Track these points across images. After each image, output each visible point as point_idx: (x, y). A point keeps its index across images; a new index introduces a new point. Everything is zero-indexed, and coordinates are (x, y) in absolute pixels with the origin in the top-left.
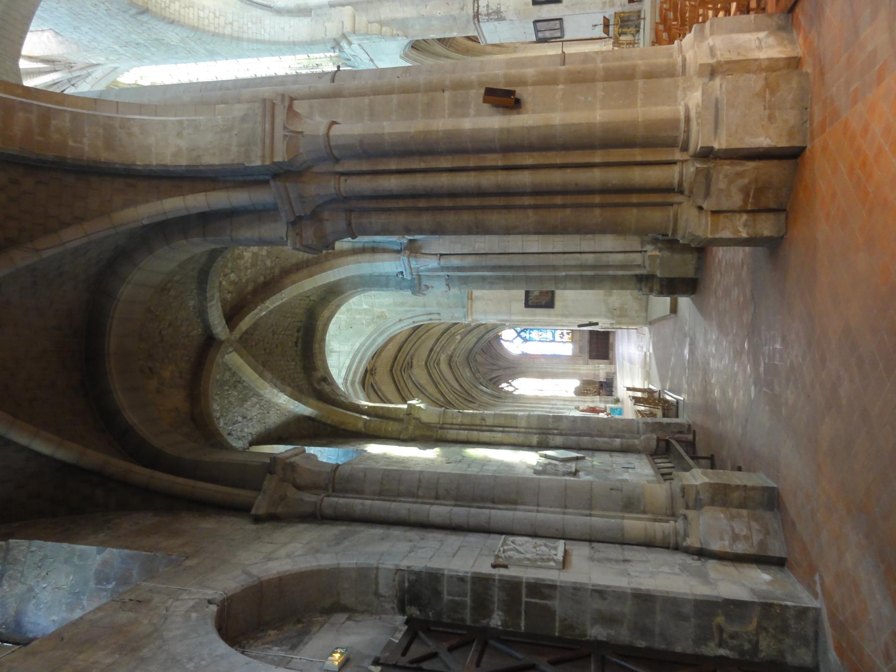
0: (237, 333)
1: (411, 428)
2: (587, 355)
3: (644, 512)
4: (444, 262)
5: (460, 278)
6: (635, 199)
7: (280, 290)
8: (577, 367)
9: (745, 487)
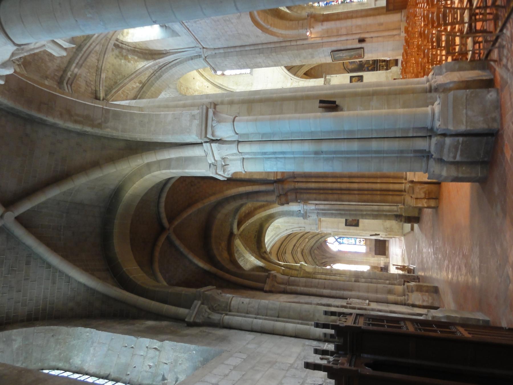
0: (239, 232)
1: (302, 273)
2: (373, 253)
3: (395, 294)
4: (317, 207)
5: (323, 213)
6: (391, 193)
7: (254, 216)
8: (368, 258)
9: (427, 286)
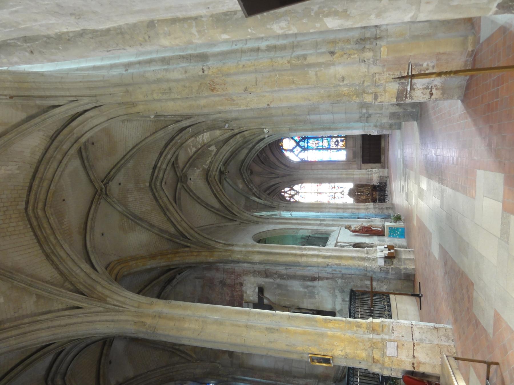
8: (350, 172)
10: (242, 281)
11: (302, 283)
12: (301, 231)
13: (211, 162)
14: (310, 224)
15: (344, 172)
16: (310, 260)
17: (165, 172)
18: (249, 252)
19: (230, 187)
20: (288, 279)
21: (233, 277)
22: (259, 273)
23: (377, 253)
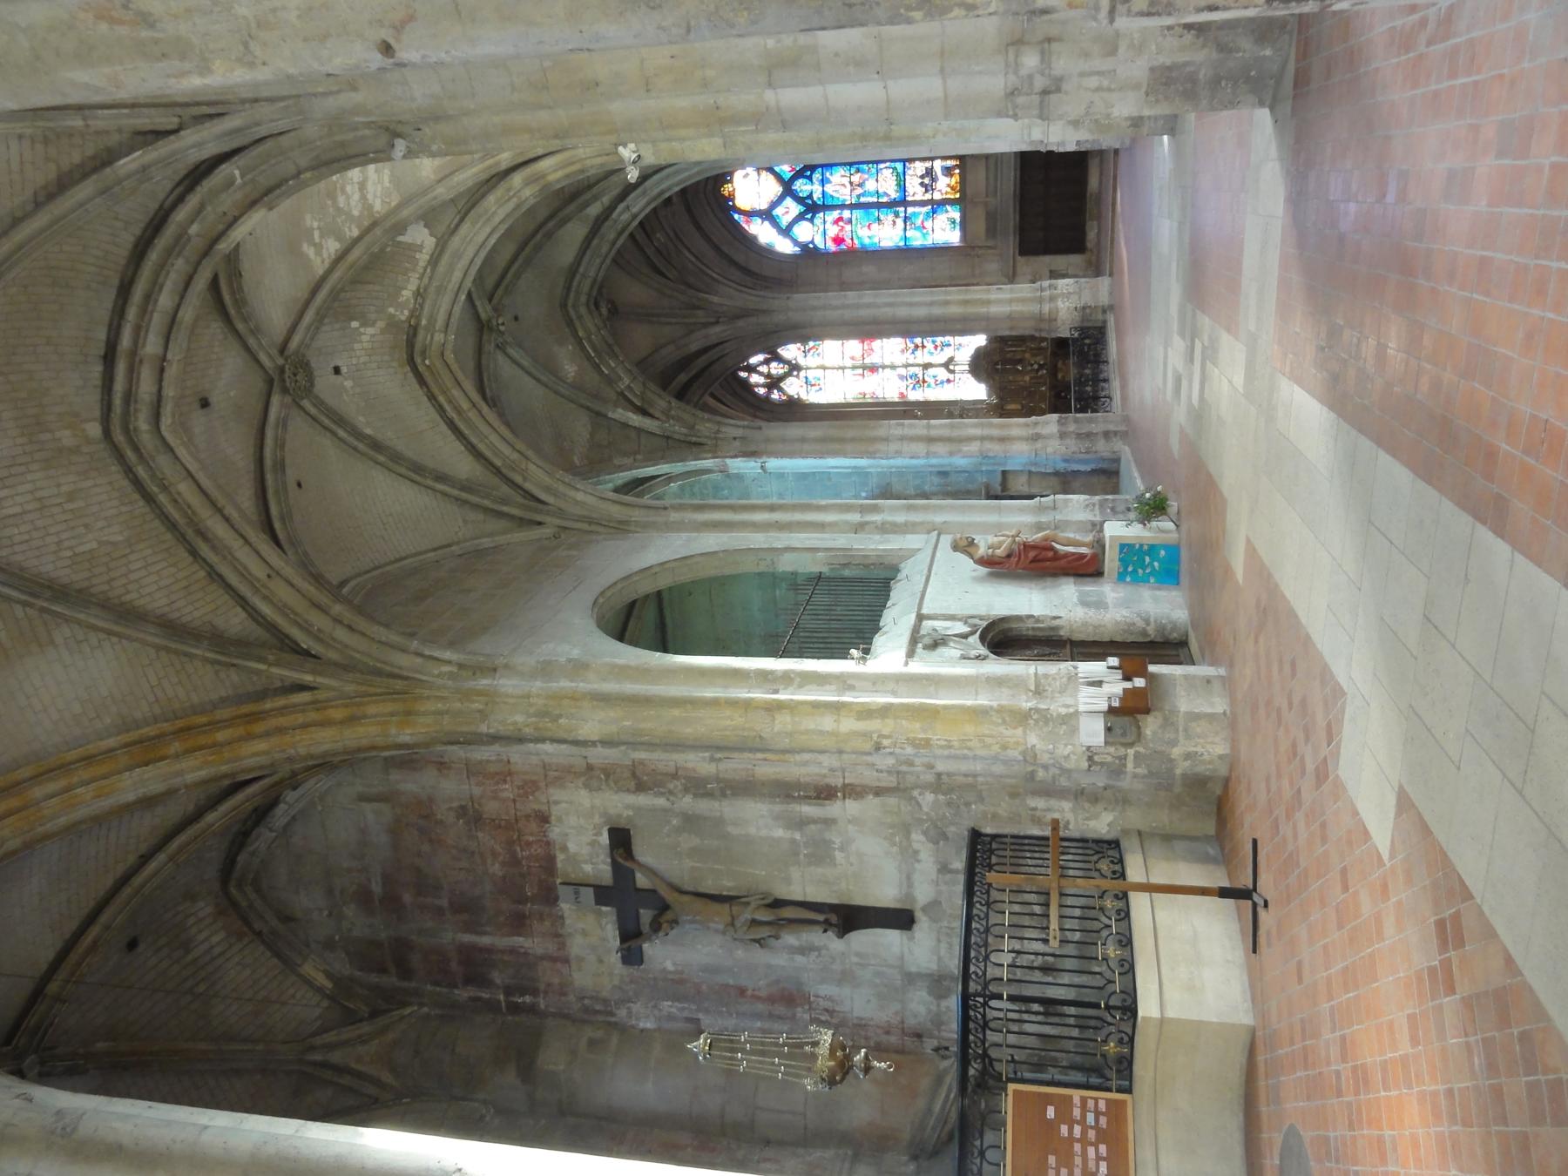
2: (1011, 243)
8: (977, 293)
10: (544, 808)
11: (778, 808)
12: (787, 556)
13: (418, 294)
14: (821, 527)
15: (955, 294)
16: (810, 723)
17: (162, 370)
18: (558, 697)
19: (527, 378)
20: (724, 795)
21: (508, 791)
22: (608, 776)
23: (1077, 690)
